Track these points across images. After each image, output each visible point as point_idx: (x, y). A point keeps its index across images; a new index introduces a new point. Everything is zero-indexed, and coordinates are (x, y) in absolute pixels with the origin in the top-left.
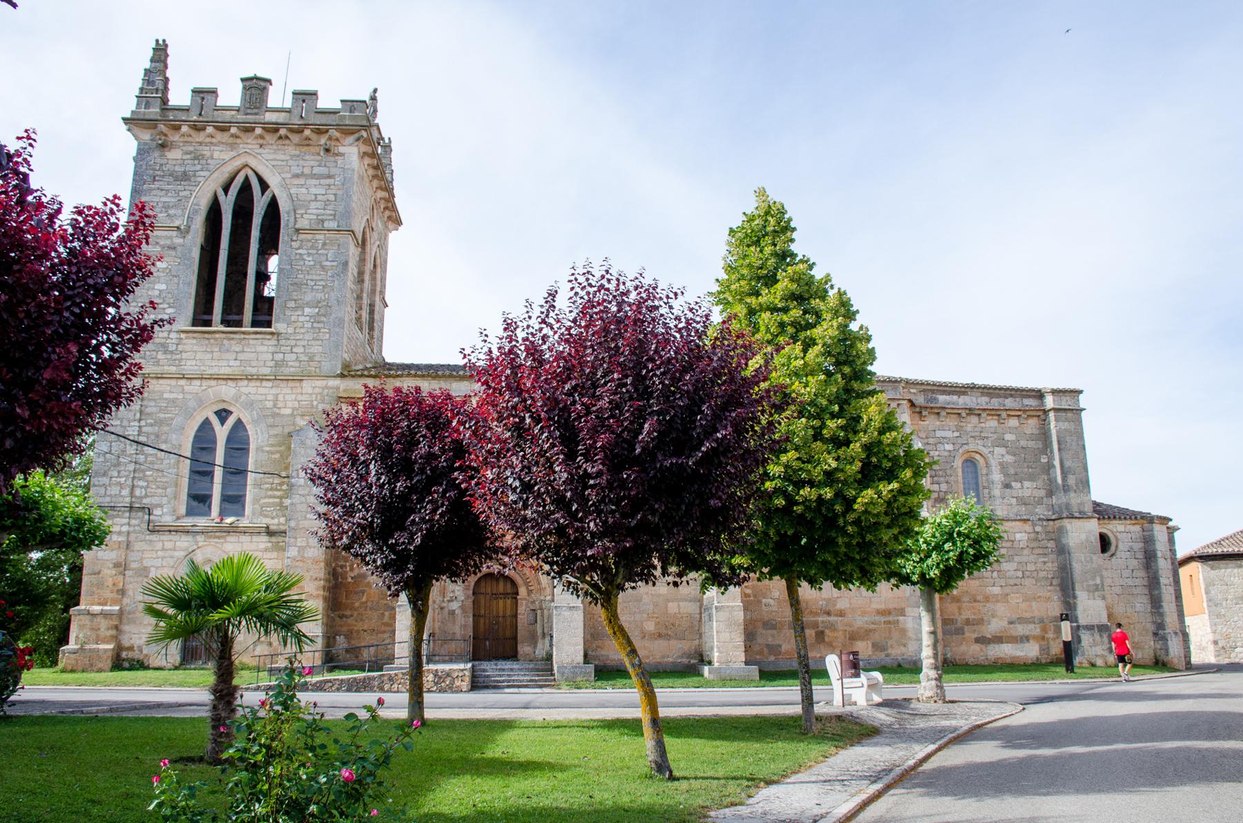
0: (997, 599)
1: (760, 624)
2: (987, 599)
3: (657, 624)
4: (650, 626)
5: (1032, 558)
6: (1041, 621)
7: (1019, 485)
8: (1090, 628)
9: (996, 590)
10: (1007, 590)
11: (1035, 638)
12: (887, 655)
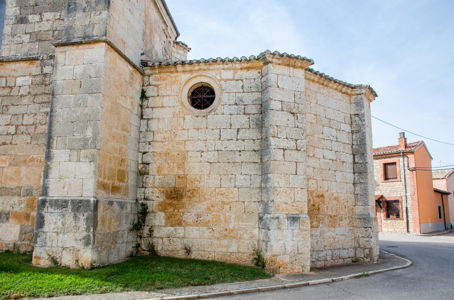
5: (33, 108)
6: (29, 193)
7: (37, 18)
8: (61, 204)
11: (17, 216)
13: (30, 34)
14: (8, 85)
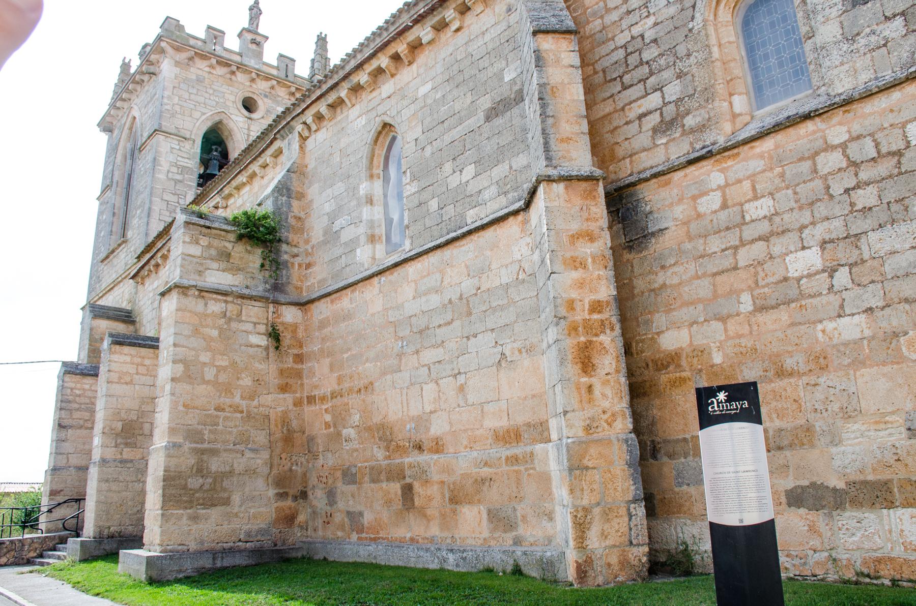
0: (856, 356)
1: (339, 474)
2: (820, 362)
9: (851, 327)
10: (896, 318)
12: (517, 542)
13: (903, 14)
14: (884, 150)
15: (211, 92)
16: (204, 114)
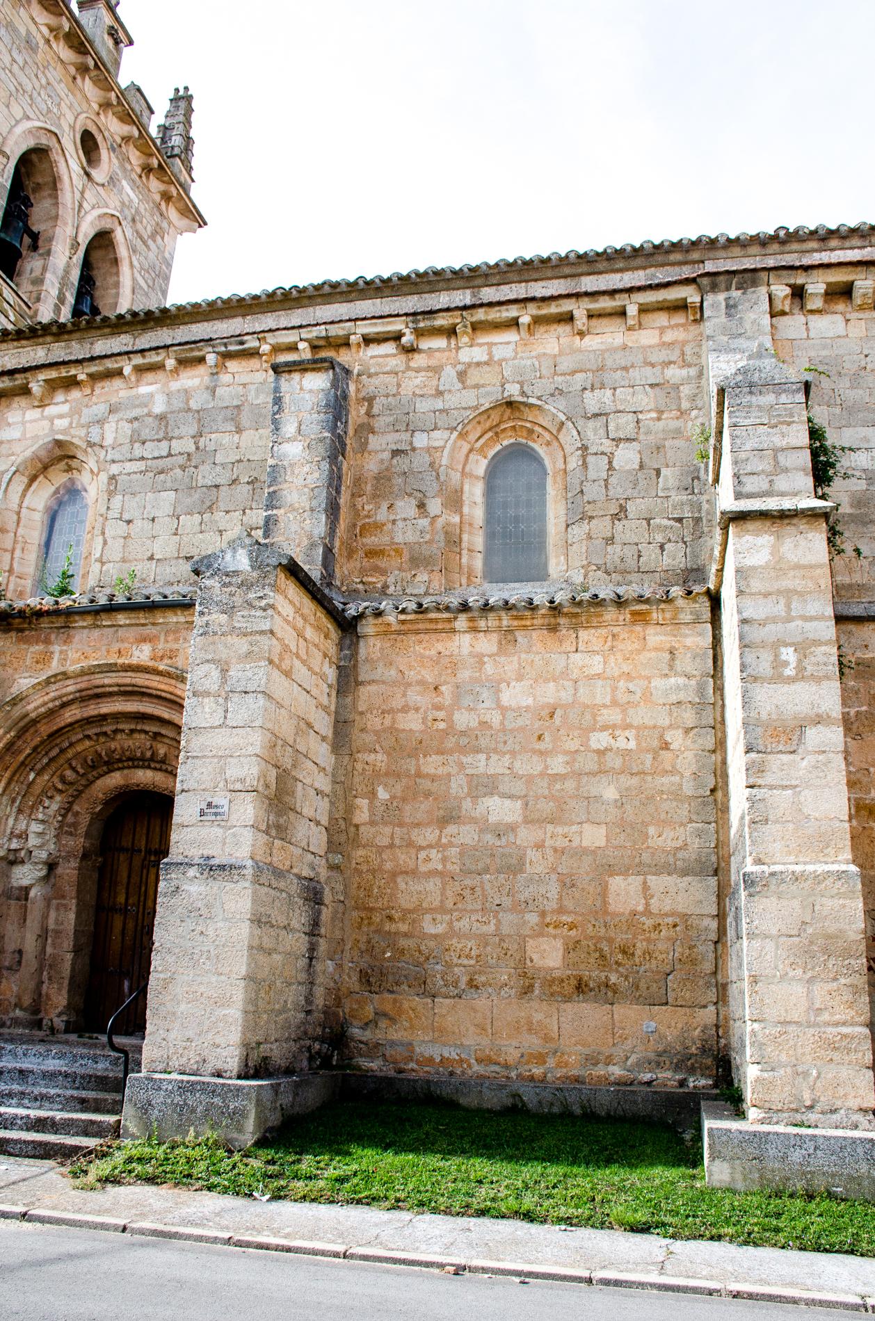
3: (571, 947)
4: (549, 955)
15: (44, 81)
16: (28, 118)
